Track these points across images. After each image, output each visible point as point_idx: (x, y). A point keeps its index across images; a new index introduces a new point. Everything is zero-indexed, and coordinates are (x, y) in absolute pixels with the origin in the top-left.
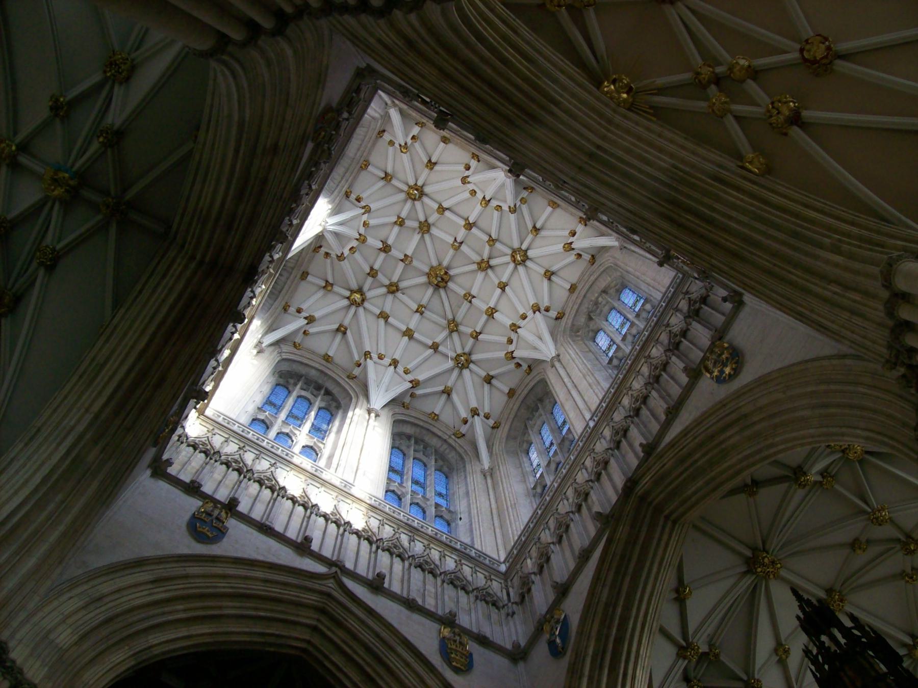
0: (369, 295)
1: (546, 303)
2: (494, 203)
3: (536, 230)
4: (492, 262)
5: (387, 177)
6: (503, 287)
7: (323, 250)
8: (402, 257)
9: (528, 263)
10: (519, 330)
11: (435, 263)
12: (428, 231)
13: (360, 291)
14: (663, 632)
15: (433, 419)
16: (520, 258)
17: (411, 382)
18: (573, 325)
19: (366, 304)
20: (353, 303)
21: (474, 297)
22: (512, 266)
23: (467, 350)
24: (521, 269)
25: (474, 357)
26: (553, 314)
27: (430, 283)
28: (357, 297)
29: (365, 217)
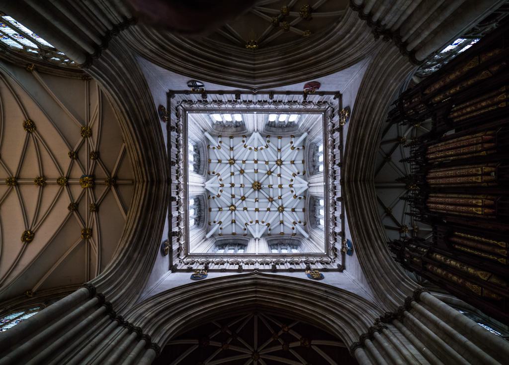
0: (236, 205)
1: (297, 171)
2: (259, 148)
3: (279, 150)
4: (272, 170)
5: (220, 161)
6: (279, 175)
7: (211, 197)
9: (283, 163)
11: (253, 182)
12: (244, 172)
13: (232, 205)
14: (388, 228)
15: (282, 235)
16: (280, 163)
18: (310, 173)
19: (237, 209)
20: (232, 210)
23: (280, 205)
24: (282, 166)
25: (284, 206)
26: (301, 174)
27: (255, 190)
28: (233, 208)
29: (219, 177)
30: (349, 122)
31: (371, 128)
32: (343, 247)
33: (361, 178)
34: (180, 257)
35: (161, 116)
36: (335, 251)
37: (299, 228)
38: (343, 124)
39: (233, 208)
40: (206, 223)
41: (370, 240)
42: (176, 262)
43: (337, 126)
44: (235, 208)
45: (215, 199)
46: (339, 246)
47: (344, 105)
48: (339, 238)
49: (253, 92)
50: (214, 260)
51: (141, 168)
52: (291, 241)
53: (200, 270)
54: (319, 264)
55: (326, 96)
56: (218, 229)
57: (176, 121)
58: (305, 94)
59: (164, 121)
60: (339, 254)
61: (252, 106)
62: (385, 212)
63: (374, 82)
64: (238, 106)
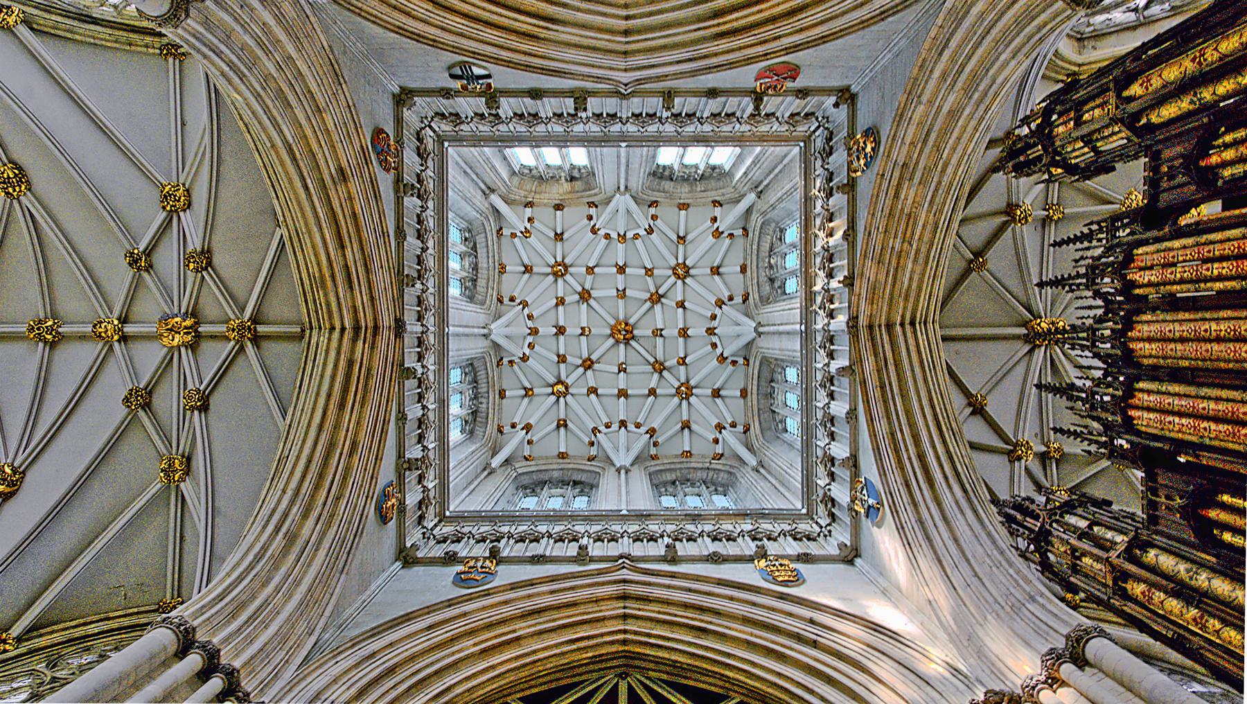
0: (569, 381)
2: (630, 235)
4: (661, 291)
5: (528, 269)
7: (505, 361)
9: (692, 272)
10: (716, 331)
11: (612, 322)
12: (590, 295)
13: (560, 382)
16: (682, 272)
17: (647, 432)
18: (760, 297)
19: (571, 390)
20: (559, 395)
21: (662, 330)
23: (683, 380)
24: (688, 280)
27: (618, 342)
28: (560, 388)
29: (526, 311)
31: (939, 183)
33: (903, 317)
36: (829, 505)
38: (859, 174)
39: (561, 390)
40: (491, 429)
43: (841, 178)
44: (567, 388)
45: (515, 366)
46: (841, 493)
47: (863, 123)
48: (843, 473)
49: (620, 92)
51: (326, 295)
52: (711, 474)
55: (813, 101)
57: (418, 169)
61: (616, 128)
62: (970, 404)
63: (952, 60)
64: (579, 128)
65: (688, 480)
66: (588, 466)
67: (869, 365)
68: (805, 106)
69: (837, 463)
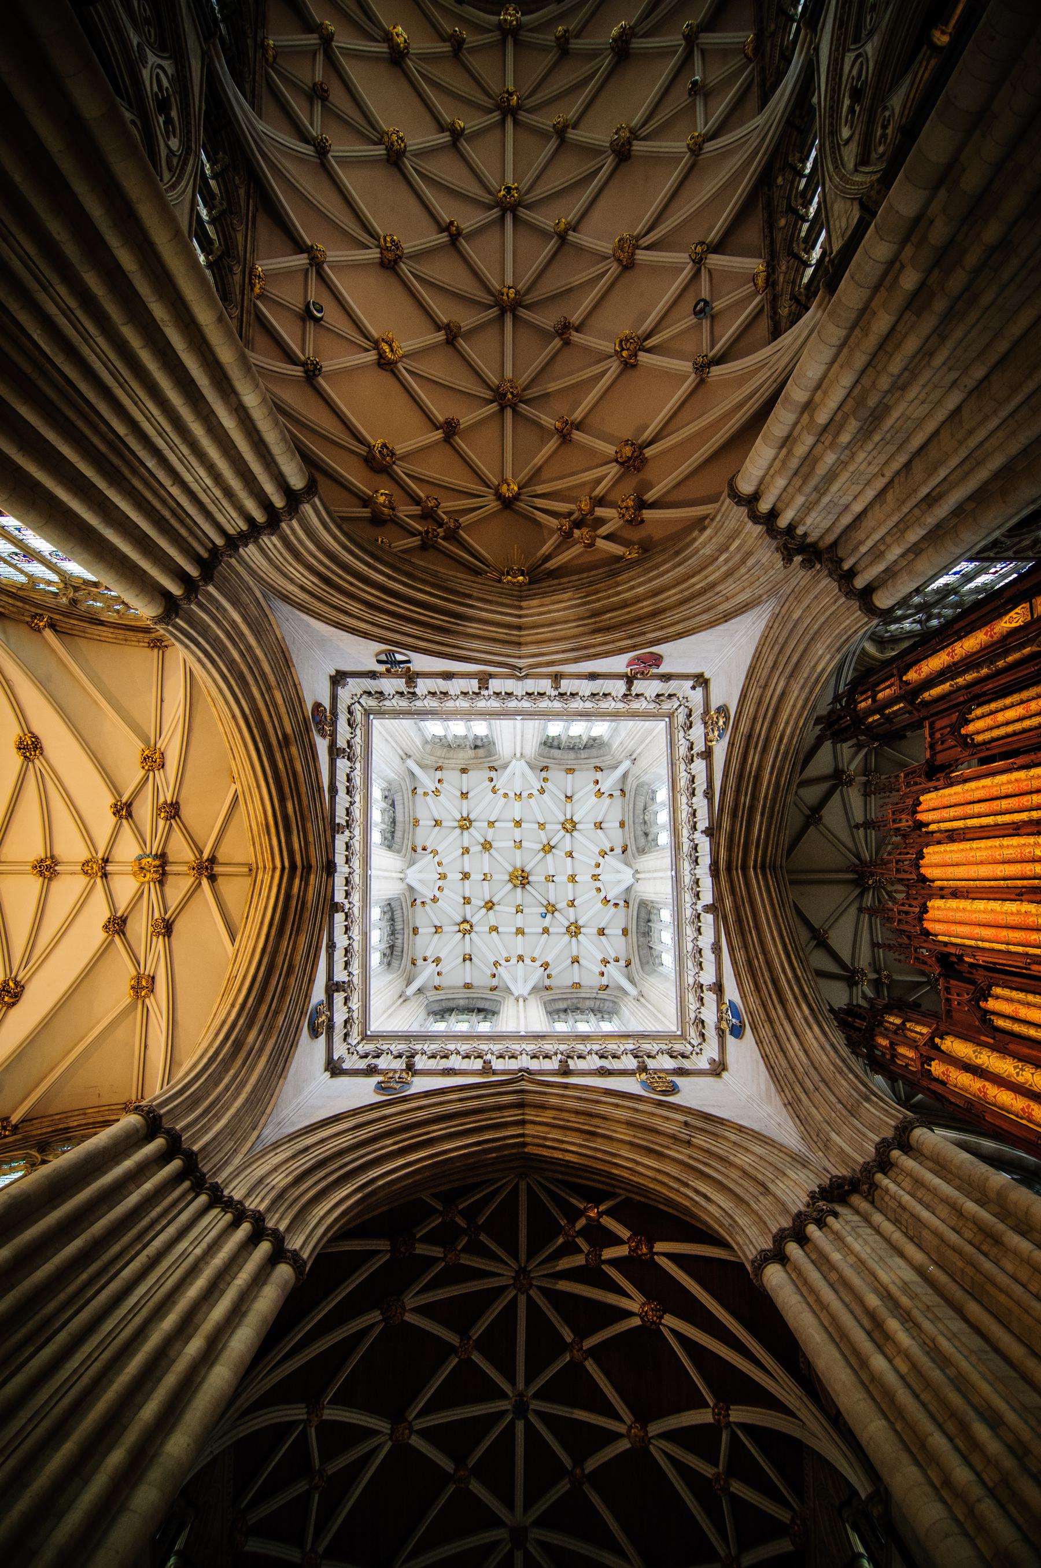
0: (474, 921)
4: (552, 843)
5: (437, 823)
6: (570, 855)
7: (418, 902)
8: (483, 877)
9: (578, 826)
11: (511, 869)
13: (465, 921)
14: (821, 974)
16: (570, 826)
18: (638, 848)
19: (475, 929)
20: (465, 932)
22: (568, 835)
24: (575, 833)
26: (618, 850)
27: (515, 886)
29: (437, 859)
30: (727, 739)
31: (778, 751)
32: (720, 1019)
33: (755, 861)
34: (349, 1041)
35: (317, 724)
37: (615, 974)
39: (466, 927)
40: (406, 961)
41: (783, 1002)
42: (340, 1050)
43: (700, 747)
45: (427, 907)
47: (715, 703)
48: (710, 997)
50: (425, 1047)
52: (598, 1003)
53: (395, 1071)
54: (667, 1056)
55: (672, 686)
56: (432, 975)
57: (348, 736)
58: (630, 680)
59: (324, 736)
60: (711, 1033)
61: (512, 704)
62: (814, 938)
64: (481, 704)
65: (578, 1009)
66: (490, 995)
67: (728, 903)
68: (668, 688)
69: (704, 988)
